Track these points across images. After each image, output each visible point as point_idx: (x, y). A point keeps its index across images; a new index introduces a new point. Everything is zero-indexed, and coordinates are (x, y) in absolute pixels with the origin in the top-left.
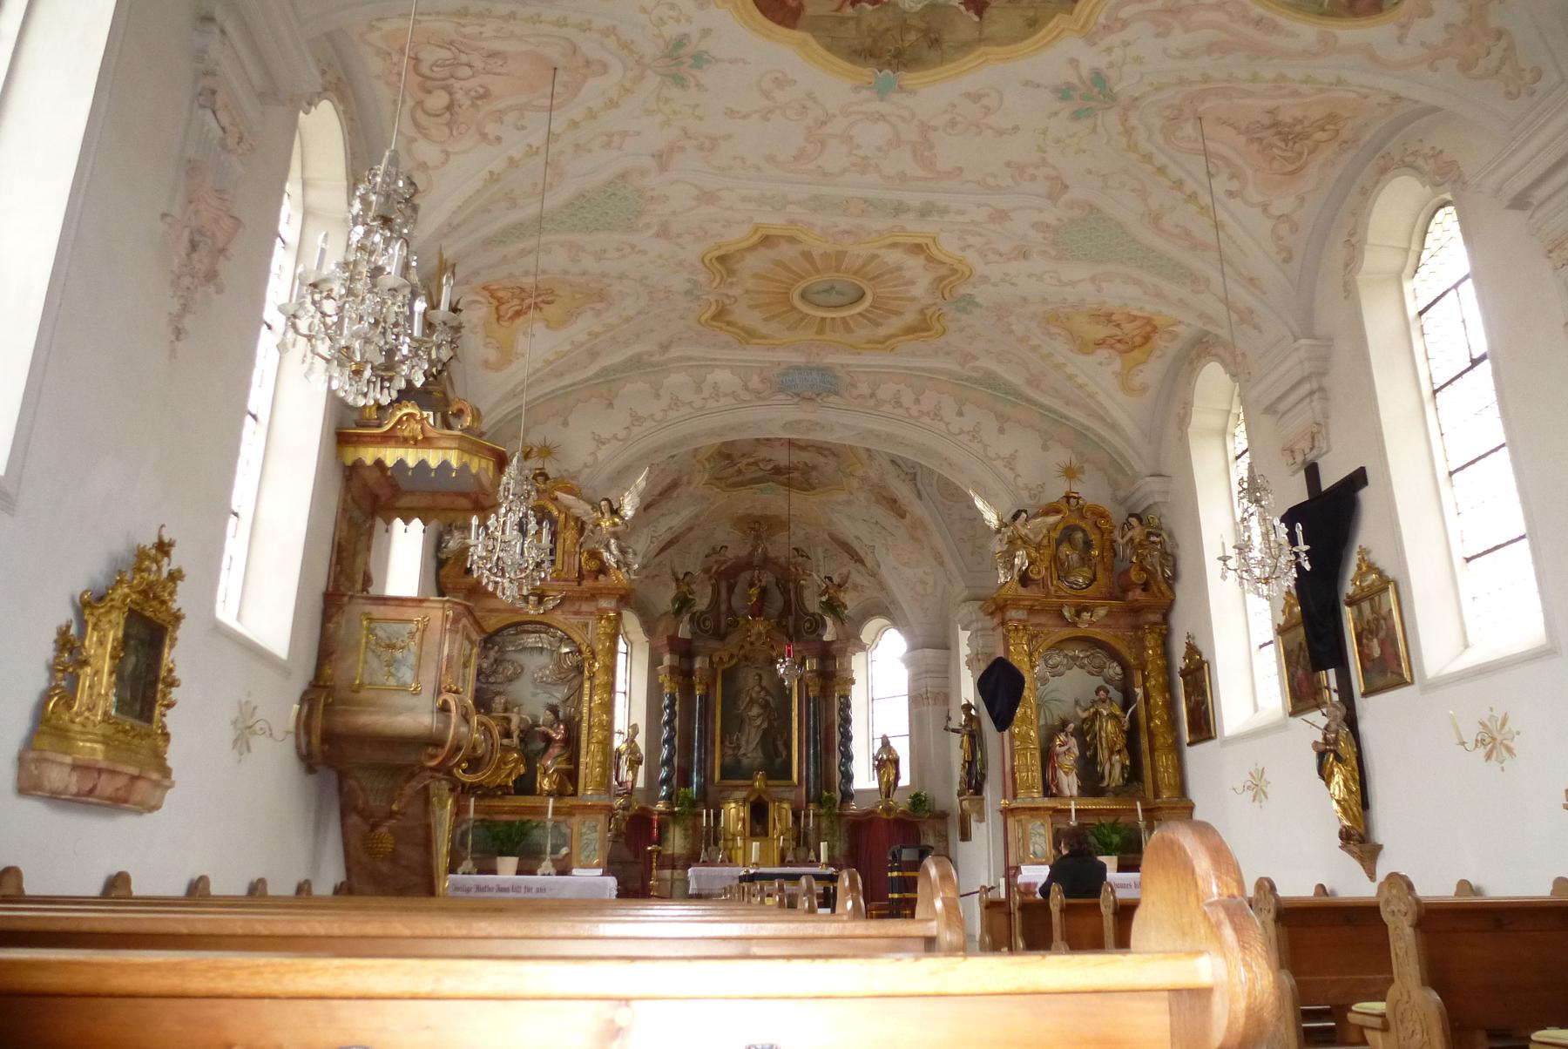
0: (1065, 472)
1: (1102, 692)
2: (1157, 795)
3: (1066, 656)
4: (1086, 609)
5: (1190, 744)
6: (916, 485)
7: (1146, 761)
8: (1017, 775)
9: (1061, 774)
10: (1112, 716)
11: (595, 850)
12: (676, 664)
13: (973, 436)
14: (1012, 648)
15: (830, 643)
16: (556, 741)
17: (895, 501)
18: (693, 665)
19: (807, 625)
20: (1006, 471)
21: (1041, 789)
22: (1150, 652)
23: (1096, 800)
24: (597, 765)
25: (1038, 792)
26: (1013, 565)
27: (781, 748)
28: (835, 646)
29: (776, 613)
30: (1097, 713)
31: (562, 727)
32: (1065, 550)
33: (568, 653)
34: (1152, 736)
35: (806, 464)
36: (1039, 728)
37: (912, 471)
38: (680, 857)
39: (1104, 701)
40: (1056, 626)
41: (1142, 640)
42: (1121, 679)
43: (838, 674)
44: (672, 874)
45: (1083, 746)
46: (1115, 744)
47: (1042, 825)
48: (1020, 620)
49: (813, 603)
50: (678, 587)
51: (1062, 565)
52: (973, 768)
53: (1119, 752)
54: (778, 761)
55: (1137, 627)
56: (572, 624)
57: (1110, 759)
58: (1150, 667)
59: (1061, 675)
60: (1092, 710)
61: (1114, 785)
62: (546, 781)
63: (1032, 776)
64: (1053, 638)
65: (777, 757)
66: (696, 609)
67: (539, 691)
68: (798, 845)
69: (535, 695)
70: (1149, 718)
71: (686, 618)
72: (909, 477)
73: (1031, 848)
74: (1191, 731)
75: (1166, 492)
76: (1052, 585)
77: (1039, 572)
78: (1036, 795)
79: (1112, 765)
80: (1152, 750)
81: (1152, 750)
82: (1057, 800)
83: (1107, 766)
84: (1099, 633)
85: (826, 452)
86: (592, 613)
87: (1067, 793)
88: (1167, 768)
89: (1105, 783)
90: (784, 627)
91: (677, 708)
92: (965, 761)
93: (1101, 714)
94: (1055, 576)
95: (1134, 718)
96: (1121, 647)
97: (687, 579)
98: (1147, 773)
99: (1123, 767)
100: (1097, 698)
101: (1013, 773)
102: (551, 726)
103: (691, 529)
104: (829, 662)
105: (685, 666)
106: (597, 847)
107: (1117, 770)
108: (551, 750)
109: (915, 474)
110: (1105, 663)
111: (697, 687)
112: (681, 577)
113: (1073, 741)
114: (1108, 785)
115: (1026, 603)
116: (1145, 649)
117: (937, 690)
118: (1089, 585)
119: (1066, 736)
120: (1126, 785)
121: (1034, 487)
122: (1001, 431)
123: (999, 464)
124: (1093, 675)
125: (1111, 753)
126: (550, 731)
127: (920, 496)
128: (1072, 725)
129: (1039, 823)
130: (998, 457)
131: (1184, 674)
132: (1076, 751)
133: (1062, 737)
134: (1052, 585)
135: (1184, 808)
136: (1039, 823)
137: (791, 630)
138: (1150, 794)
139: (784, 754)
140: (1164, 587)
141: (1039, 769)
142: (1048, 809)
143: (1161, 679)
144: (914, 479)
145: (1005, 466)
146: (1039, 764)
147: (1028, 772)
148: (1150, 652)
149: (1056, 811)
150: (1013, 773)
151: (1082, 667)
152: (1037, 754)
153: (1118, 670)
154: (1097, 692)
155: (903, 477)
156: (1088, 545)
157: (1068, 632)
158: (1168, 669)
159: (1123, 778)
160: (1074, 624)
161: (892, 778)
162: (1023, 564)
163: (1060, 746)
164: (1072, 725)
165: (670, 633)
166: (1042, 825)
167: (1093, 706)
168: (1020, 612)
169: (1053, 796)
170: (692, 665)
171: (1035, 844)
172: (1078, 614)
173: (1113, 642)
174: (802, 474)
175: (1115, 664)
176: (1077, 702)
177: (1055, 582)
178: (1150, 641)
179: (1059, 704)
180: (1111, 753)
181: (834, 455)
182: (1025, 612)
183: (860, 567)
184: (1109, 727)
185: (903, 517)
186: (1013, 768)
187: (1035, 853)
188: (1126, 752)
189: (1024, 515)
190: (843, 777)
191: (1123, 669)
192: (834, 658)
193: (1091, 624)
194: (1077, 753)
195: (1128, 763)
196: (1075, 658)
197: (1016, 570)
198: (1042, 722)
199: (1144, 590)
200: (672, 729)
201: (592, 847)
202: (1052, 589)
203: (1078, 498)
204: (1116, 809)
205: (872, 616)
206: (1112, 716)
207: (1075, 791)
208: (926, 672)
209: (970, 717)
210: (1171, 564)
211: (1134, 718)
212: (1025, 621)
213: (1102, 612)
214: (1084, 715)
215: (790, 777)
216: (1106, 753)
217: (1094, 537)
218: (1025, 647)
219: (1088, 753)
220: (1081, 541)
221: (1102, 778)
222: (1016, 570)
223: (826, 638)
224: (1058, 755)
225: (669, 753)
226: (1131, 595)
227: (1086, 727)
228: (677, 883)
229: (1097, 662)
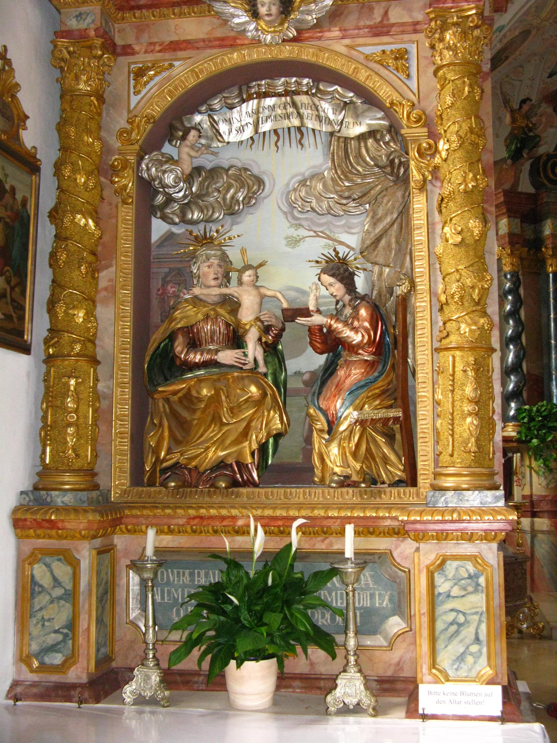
11: (477, 639)
12: (517, 231)
16: (352, 349)
18: (541, 232)
24: (468, 408)
31: (363, 312)
33: (362, 137)
38: (543, 498)
44: (532, 524)
50: (514, 120)
56: (367, 57)
62: (334, 450)
66: (542, 150)
67: (303, 232)
69: (294, 242)
71: (527, 167)
86: (415, 27)
91: (522, 291)
97: (526, 107)
102: (337, 315)
103: (526, 34)
105: (529, 234)
106: (483, 636)
108: (341, 373)
111: (549, 262)
112: (516, 106)
126: (339, 326)
165: (507, 186)
170: (538, 232)
200: (518, 322)
201: (468, 632)
225: (517, 356)
228: (540, 536)
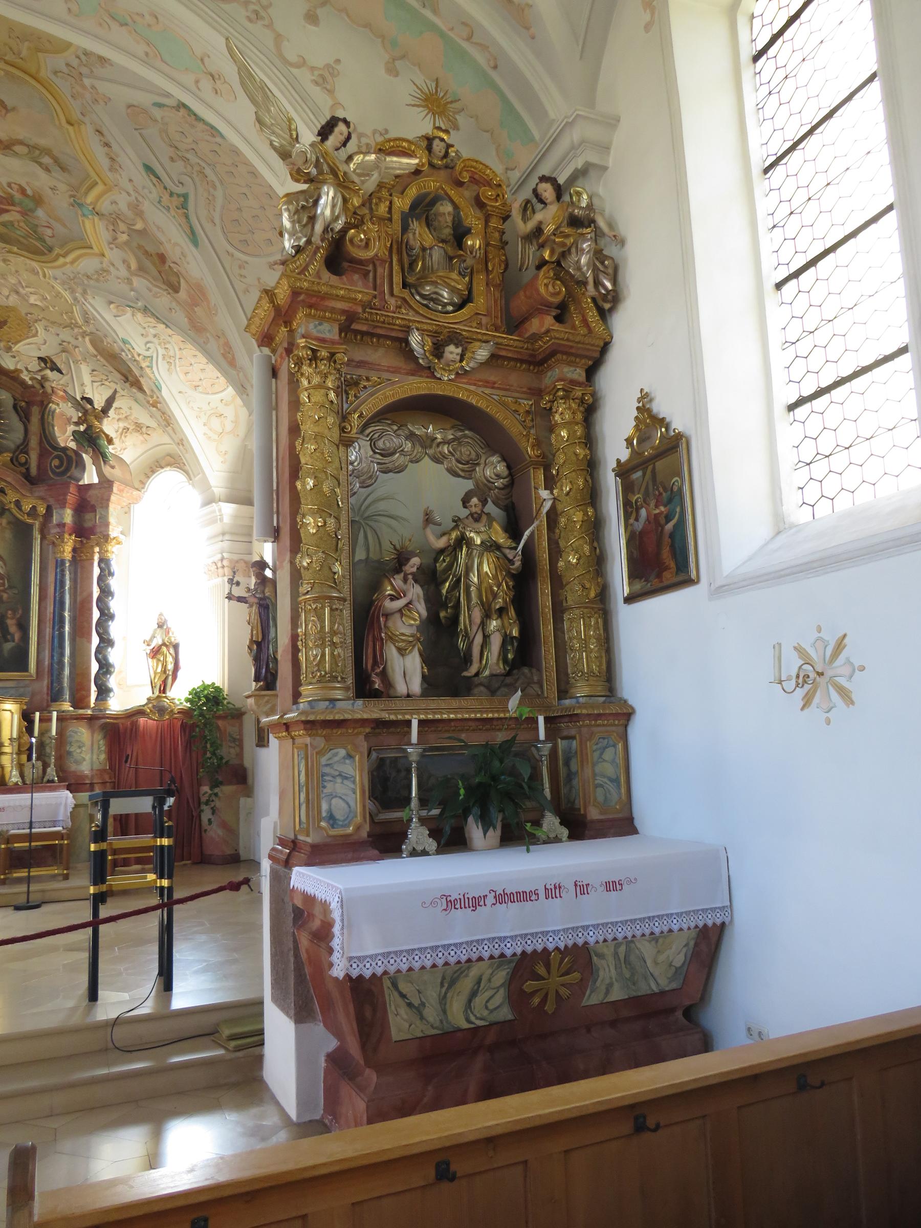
0: (426, 100)
1: (475, 500)
2: (563, 693)
3: (411, 436)
4: (455, 338)
5: (629, 600)
6: (187, 217)
7: (546, 629)
8: (302, 657)
9: (391, 652)
10: (491, 547)
13: (256, 13)
14: (304, 397)
15: (90, 486)
17: (162, 258)
19: (56, 462)
20: (316, 93)
21: (350, 681)
22: (564, 433)
23: (455, 702)
25: (347, 689)
26: (312, 219)
27: (13, 629)
28: (91, 493)
29: (13, 446)
30: (462, 541)
32: (420, 235)
34: (557, 582)
35: (23, 191)
36: (353, 565)
37: (180, 190)
39: (476, 518)
40: (395, 371)
41: (549, 411)
42: (505, 487)
43: (98, 530)
45: (434, 602)
46: (495, 596)
47: (350, 756)
48: (322, 340)
49: (65, 437)
51: (412, 264)
52: (264, 649)
53: (501, 612)
54: (8, 646)
55: (537, 393)
57: (483, 625)
58: (561, 458)
59: (400, 470)
60: (454, 535)
61: (487, 673)
63: (332, 654)
64: (389, 392)
65: (7, 641)
68: (29, 758)
70: (556, 552)
72: (176, 201)
73: (324, 806)
74: (633, 575)
75: (605, 148)
76: (392, 294)
77: (367, 245)
78: (339, 694)
79: (486, 637)
80: (559, 610)
81: (559, 610)
82: (382, 703)
83: (479, 639)
84: (465, 393)
85: (46, 160)
87: (401, 688)
88: (586, 641)
89: (473, 669)
90: (22, 465)
92: (252, 641)
93: (469, 543)
94: (397, 279)
95: (528, 555)
96: (512, 425)
98: (547, 653)
99: (507, 640)
100: (463, 513)
101: (295, 650)
104: (88, 516)
107: (496, 642)
109: (185, 196)
110: (478, 456)
113: (415, 592)
114: (477, 674)
115: (339, 305)
116: (552, 429)
117: (236, 557)
118: (460, 307)
119: (405, 580)
120: (509, 674)
121: (369, 132)
122: (312, 18)
123: (305, 77)
124: (456, 475)
125: (487, 616)
127: (194, 239)
128: (415, 561)
129: (342, 752)
130: (302, 63)
131: (623, 471)
132: (421, 608)
133: (397, 581)
134: (392, 294)
135: (616, 715)
136: (342, 752)
137: (34, 471)
138: (551, 690)
139: (17, 637)
140: (592, 315)
141: (349, 641)
142: (363, 722)
143: (581, 482)
144: (184, 206)
145: (316, 83)
146: (349, 633)
147: (323, 646)
148: (564, 433)
149: (380, 724)
150: (295, 650)
151: (437, 460)
152: (347, 613)
153: (501, 468)
154: (465, 502)
155: (166, 197)
156: (460, 234)
157: (418, 386)
158: (591, 466)
159: (505, 661)
160: (430, 371)
161: (170, 667)
162: (335, 219)
163: (393, 598)
164: (415, 561)
166: (350, 756)
167: (456, 527)
168: (326, 326)
169: (375, 694)
171: (332, 796)
172: (438, 351)
173: (500, 415)
174: (24, 213)
175: (495, 459)
176: (428, 519)
177: (396, 290)
178: (562, 413)
179: (393, 522)
180: (487, 616)
181: (63, 169)
182: (336, 330)
183: (139, 395)
184: (486, 568)
185: (176, 290)
186: (294, 638)
187: (331, 818)
188: (512, 612)
189: (341, 127)
190: (101, 668)
191: (509, 467)
192: (93, 509)
193: (462, 374)
194: (424, 613)
195: (515, 633)
196: (427, 442)
197: (319, 227)
198: (360, 555)
199: (559, 319)
202: (392, 302)
203: (449, 146)
204: (492, 719)
205: (162, 468)
206: (491, 547)
207: (416, 686)
208: (223, 534)
209: (263, 580)
210: (610, 271)
211: (528, 555)
212: (333, 342)
213: (482, 353)
214: (441, 543)
215: (24, 667)
216: (477, 615)
217: (472, 218)
218: (332, 395)
219: (442, 614)
220: (449, 219)
221: (467, 659)
222: (319, 227)
223: (86, 480)
224: (387, 616)
226: (535, 325)
227: (441, 566)
229: (466, 451)
